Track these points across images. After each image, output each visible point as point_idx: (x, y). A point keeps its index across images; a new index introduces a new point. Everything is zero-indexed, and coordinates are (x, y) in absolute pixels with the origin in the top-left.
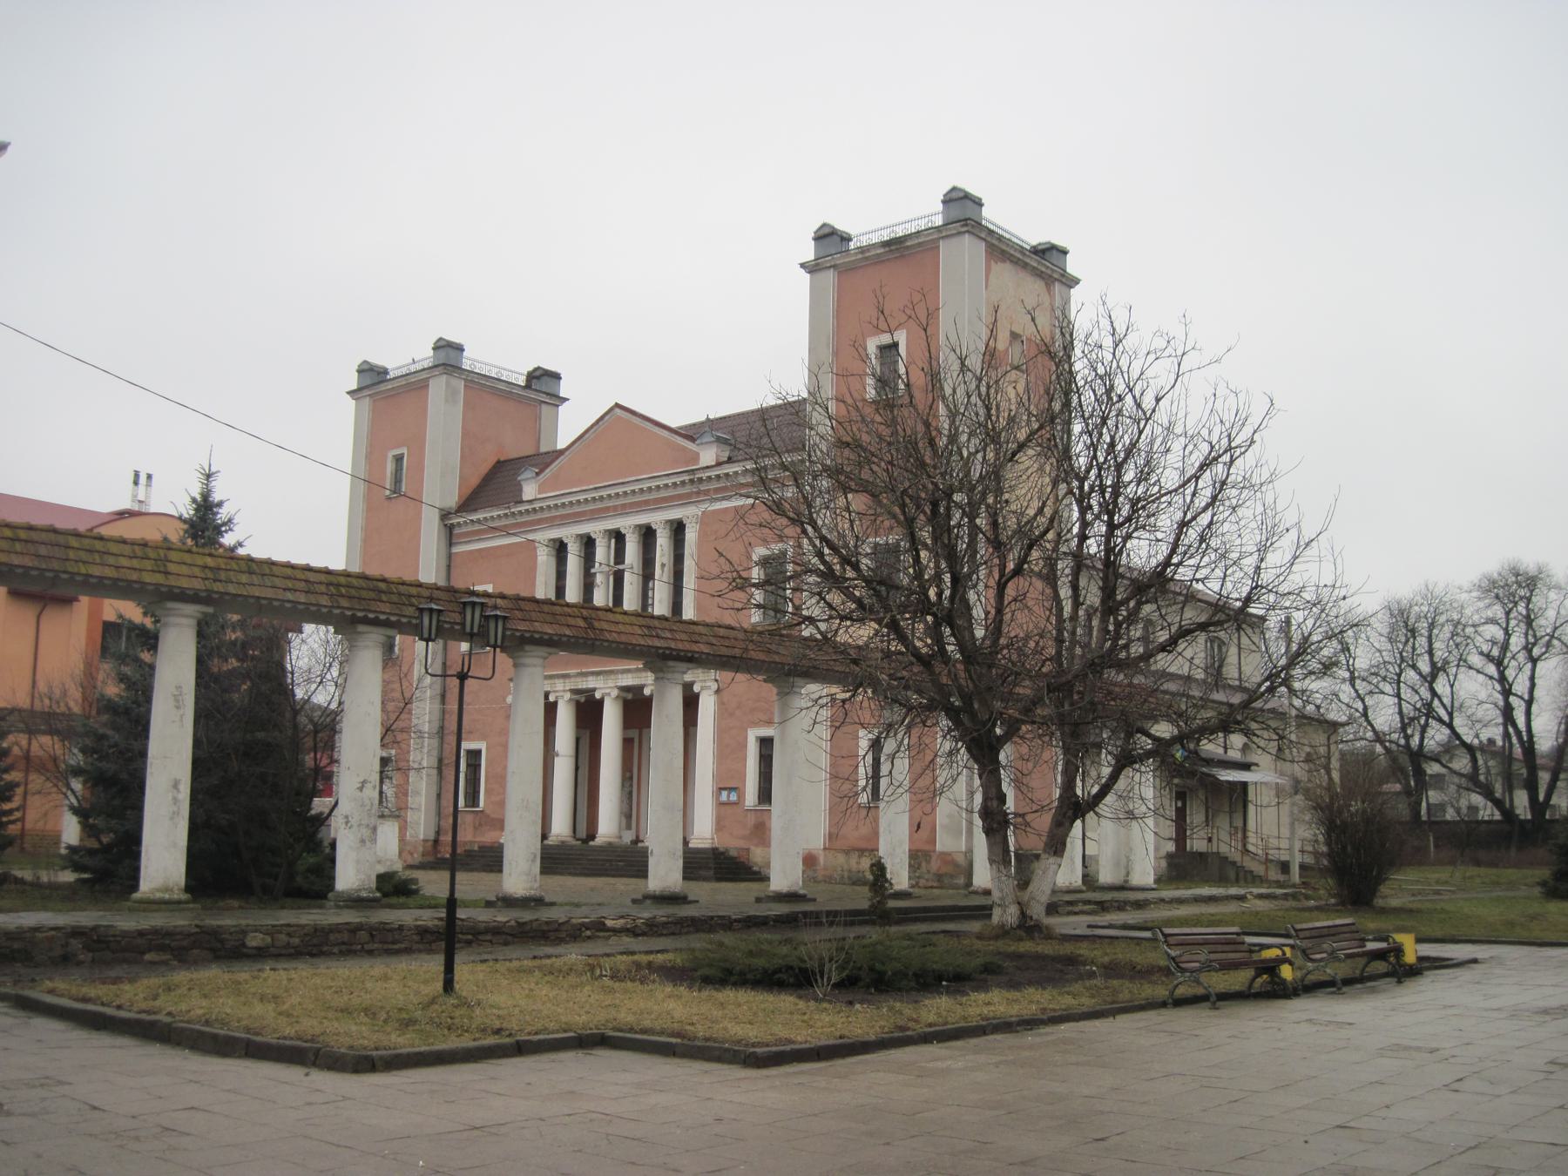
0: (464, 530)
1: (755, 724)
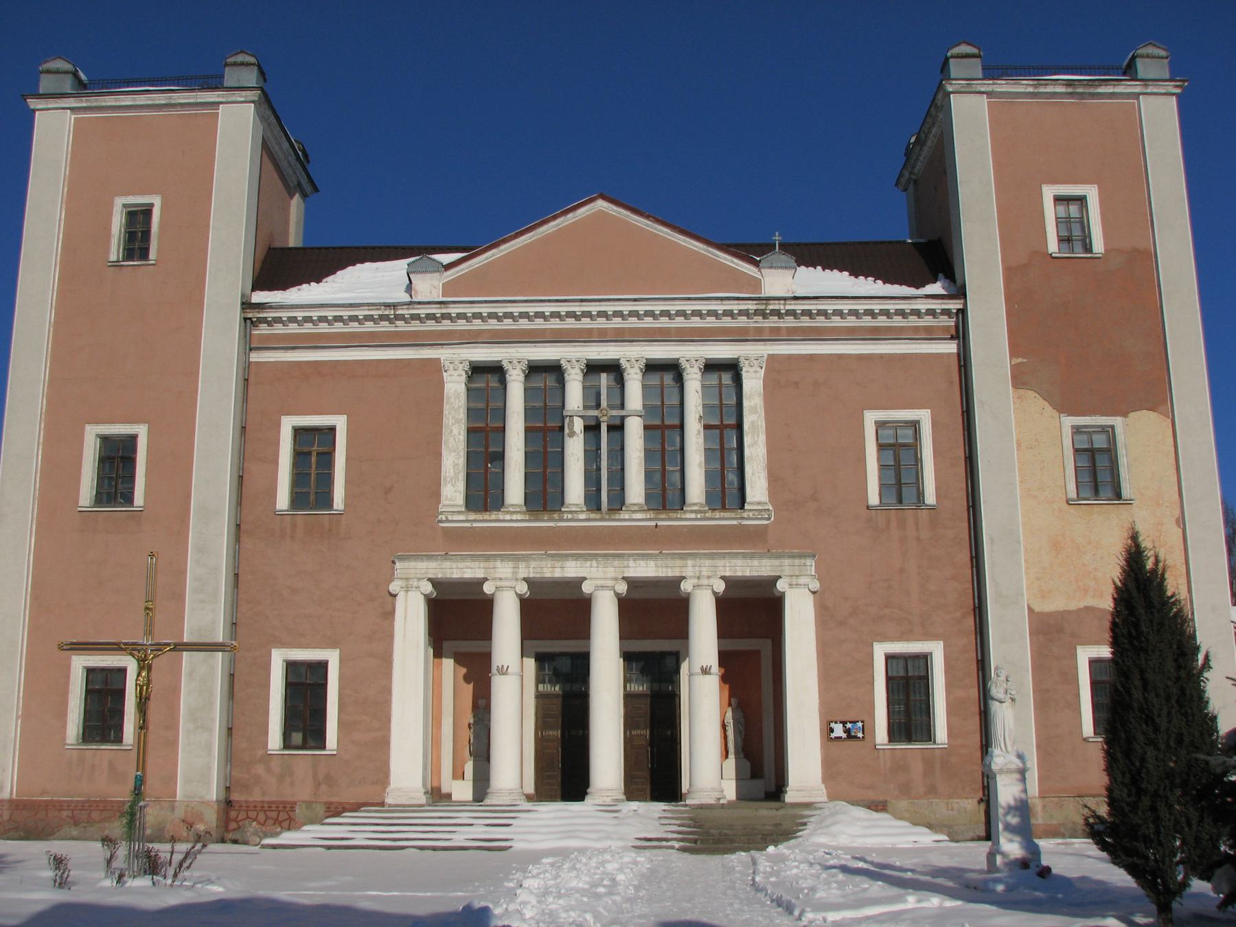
0: (279, 329)
1: (885, 638)
